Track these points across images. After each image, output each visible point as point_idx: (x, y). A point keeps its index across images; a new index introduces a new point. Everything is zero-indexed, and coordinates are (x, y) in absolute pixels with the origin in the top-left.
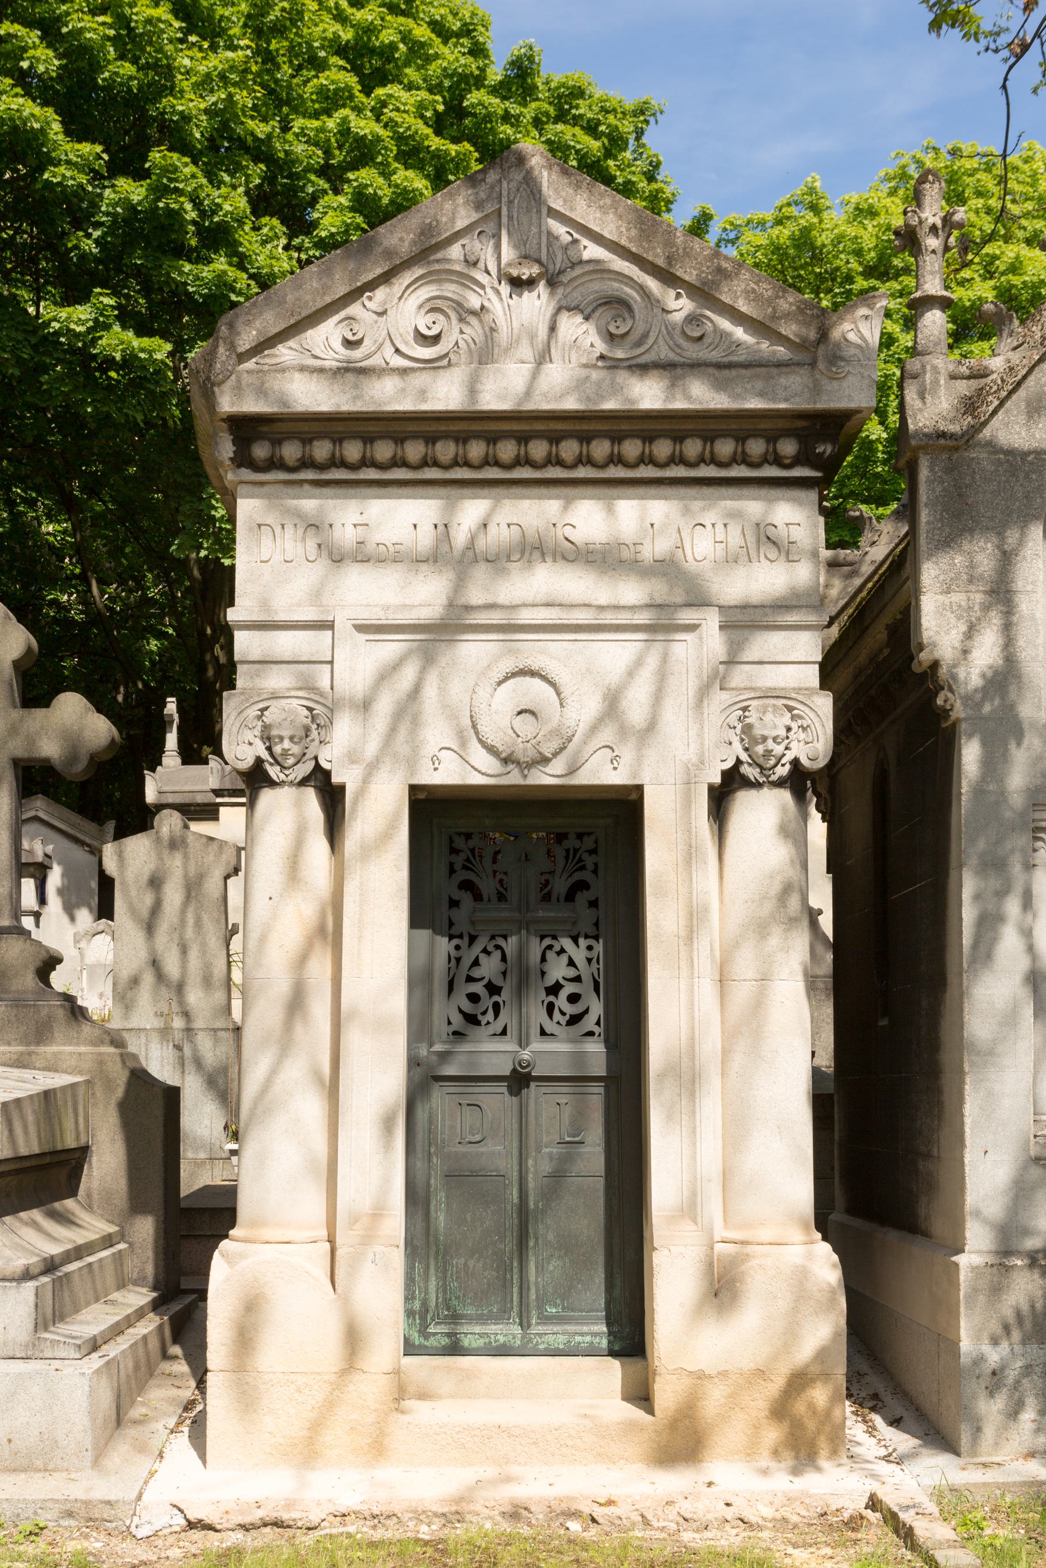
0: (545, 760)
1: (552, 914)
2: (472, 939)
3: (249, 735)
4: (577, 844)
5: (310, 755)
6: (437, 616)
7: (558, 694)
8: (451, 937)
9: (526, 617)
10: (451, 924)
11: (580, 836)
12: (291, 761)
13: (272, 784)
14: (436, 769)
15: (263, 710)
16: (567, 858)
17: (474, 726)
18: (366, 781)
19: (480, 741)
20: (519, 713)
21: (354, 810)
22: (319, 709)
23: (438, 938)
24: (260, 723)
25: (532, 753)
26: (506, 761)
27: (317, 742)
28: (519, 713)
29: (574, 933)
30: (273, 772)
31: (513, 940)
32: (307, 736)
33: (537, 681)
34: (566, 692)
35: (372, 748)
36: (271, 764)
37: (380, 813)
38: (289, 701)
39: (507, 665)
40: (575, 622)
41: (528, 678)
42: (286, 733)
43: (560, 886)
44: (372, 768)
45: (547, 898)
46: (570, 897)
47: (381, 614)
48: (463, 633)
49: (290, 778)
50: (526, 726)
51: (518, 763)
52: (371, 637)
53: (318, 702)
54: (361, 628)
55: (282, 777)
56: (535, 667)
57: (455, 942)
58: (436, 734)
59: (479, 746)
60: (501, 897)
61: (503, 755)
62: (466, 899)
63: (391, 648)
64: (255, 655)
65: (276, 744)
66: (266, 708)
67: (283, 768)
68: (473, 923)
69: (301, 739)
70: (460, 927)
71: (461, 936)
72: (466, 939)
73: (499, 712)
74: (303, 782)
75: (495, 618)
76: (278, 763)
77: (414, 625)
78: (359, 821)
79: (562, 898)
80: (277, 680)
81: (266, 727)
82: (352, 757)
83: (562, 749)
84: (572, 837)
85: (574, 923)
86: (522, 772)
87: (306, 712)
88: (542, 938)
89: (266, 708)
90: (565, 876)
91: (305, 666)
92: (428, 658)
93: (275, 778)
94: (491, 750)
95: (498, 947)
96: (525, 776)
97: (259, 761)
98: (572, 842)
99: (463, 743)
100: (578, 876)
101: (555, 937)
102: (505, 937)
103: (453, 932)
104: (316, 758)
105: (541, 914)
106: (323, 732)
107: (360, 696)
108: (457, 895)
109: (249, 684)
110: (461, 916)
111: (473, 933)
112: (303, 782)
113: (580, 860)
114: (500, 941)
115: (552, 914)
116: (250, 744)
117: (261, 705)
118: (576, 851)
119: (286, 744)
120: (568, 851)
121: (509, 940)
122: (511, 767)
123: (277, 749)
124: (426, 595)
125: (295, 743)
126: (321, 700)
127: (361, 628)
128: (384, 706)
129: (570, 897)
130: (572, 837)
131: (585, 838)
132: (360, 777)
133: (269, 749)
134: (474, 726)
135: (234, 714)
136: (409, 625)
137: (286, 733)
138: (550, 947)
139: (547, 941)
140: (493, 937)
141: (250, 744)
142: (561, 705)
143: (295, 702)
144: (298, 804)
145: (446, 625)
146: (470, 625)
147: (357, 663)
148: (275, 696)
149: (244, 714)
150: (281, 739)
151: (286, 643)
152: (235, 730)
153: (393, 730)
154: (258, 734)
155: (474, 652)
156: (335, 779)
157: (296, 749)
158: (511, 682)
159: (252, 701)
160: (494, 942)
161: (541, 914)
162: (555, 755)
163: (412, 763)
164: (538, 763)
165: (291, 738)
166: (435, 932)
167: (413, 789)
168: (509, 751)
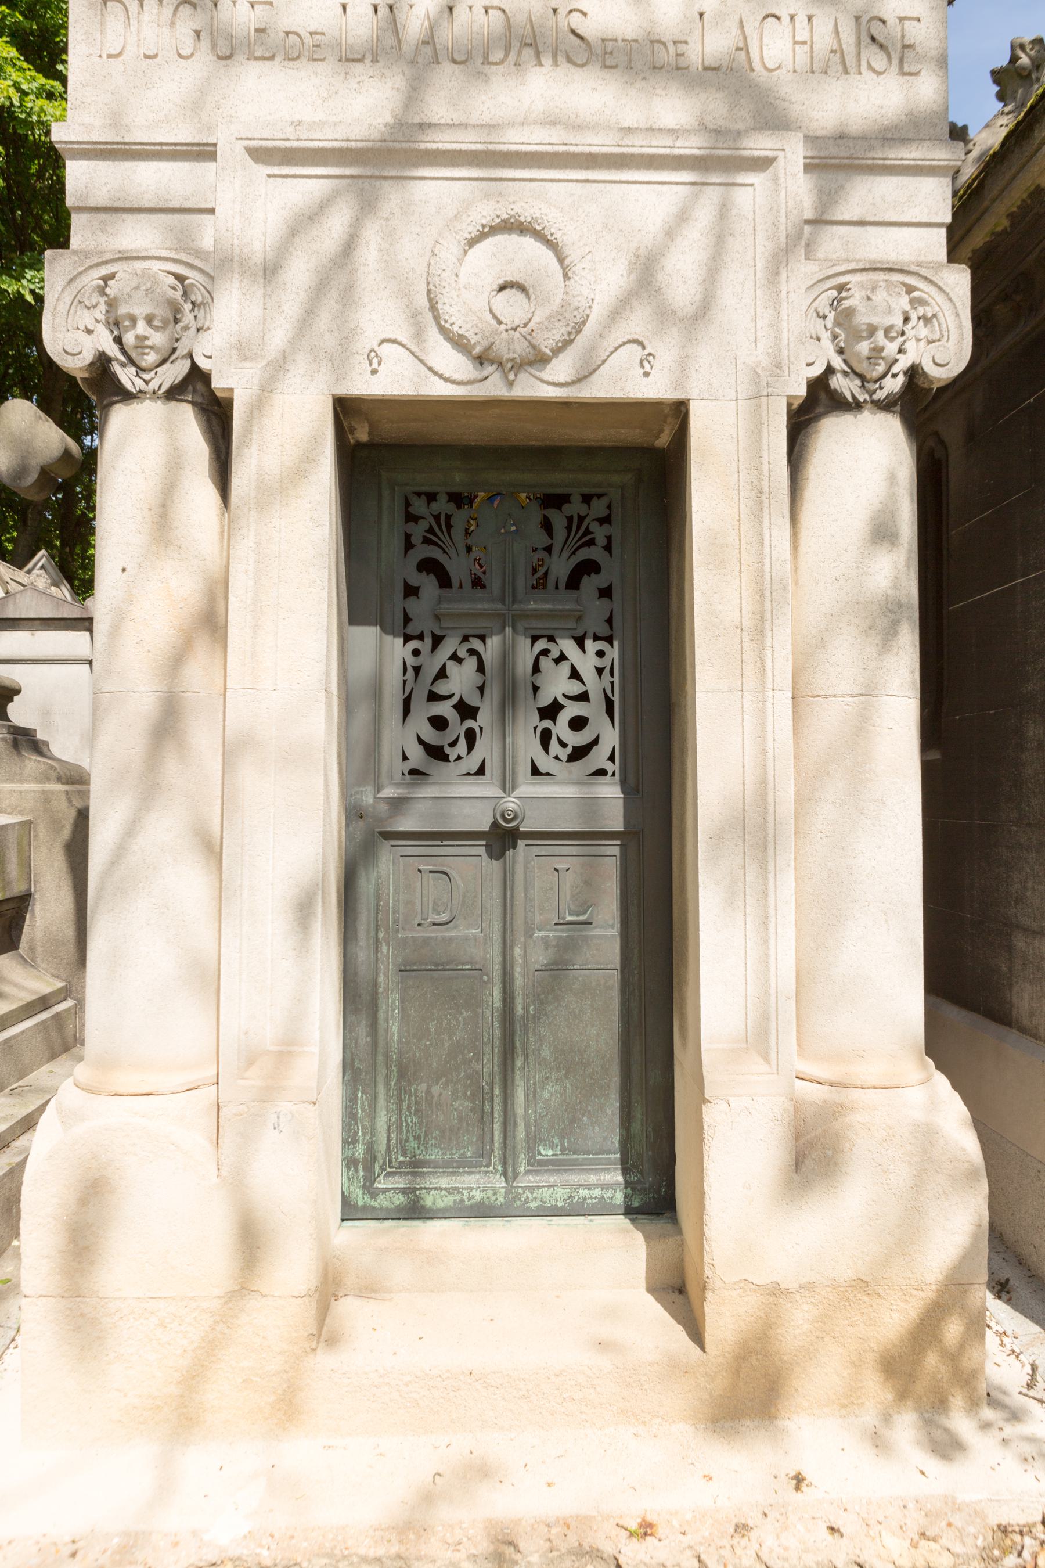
0: (540, 360)
1: (548, 606)
2: (437, 641)
3: (86, 319)
4: (583, 509)
5: (181, 351)
6: (376, 135)
7: (561, 260)
8: (407, 638)
9: (516, 140)
10: (407, 620)
11: (587, 499)
12: (151, 358)
13: (128, 396)
14: (374, 372)
15: (107, 279)
16: (569, 528)
17: (433, 307)
18: (266, 390)
19: (443, 330)
20: (502, 288)
21: (248, 431)
22: (194, 277)
23: (389, 638)
24: (103, 300)
25: (520, 348)
26: (481, 360)
27: (193, 330)
28: (502, 288)
29: (579, 633)
30: (126, 376)
31: (494, 642)
32: (176, 321)
33: (528, 241)
34: (573, 256)
35: (279, 337)
36: (123, 365)
37: (291, 440)
38: (147, 264)
39: (486, 212)
40: (587, 149)
41: (515, 237)
42: (140, 310)
43: (560, 567)
44: (279, 366)
45: (541, 584)
46: (573, 583)
47: (290, 132)
48: (416, 165)
49: (154, 385)
50: (512, 308)
51: (500, 364)
52: (276, 170)
53: (192, 266)
54: (260, 155)
55: (139, 384)
56: (526, 216)
57: (413, 644)
58: (379, 316)
59: (440, 338)
60: (477, 583)
61: (477, 350)
62: (428, 584)
63: (305, 187)
64: (100, 199)
65: (127, 331)
66: (112, 276)
67: (140, 369)
68: (437, 618)
69: (165, 323)
70: (422, 623)
71: (421, 637)
72: (428, 640)
73: (471, 290)
74: (174, 393)
75: (467, 141)
76: (134, 364)
77: (341, 150)
78: (254, 448)
79: (562, 585)
80: (137, 235)
81: (112, 304)
82: (243, 351)
83: (568, 343)
84: (576, 499)
85: (579, 618)
86: (505, 376)
87: (171, 280)
88: (535, 639)
89: (112, 276)
90: (566, 554)
91: (177, 217)
92: (367, 205)
93: (128, 386)
94: (459, 343)
95: (472, 652)
96: (511, 384)
97: (102, 362)
98: (575, 507)
99: (419, 334)
100: (584, 554)
101: (551, 639)
102: (482, 638)
103: (411, 630)
104: (191, 356)
105: (532, 605)
106: (201, 314)
107: (258, 258)
108: (416, 579)
109: (90, 244)
110: (421, 608)
111: (438, 632)
112: (174, 393)
113: (588, 532)
114: (476, 644)
115: (548, 606)
116: (89, 332)
117: (104, 271)
118: (581, 519)
119: (141, 328)
120: (570, 519)
121: (488, 641)
122: (489, 369)
123: (129, 339)
124: (363, 106)
125: (156, 329)
126: (197, 263)
127: (260, 155)
128: (299, 272)
129: (573, 583)
130: (576, 499)
131: (595, 502)
132: (256, 381)
133: (118, 340)
134: (433, 307)
135: (60, 283)
136: (333, 150)
137: (140, 310)
138: (545, 652)
139: (541, 644)
140: (466, 639)
141: (89, 332)
142: (566, 277)
143: (156, 266)
144: (170, 428)
145: (390, 151)
146: (427, 153)
147: (250, 208)
148: (126, 258)
149: (78, 284)
150: (133, 320)
151: (149, 179)
152: (63, 308)
153: (309, 313)
154: (101, 317)
155: (438, 197)
156: (216, 383)
157: (158, 338)
158: (490, 241)
159: (88, 263)
160: (466, 646)
161: (532, 605)
162: (557, 351)
163: (339, 361)
164: (531, 363)
165: (149, 320)
166: (384, 630)
167: (345, 409)
168: (485, 343)
